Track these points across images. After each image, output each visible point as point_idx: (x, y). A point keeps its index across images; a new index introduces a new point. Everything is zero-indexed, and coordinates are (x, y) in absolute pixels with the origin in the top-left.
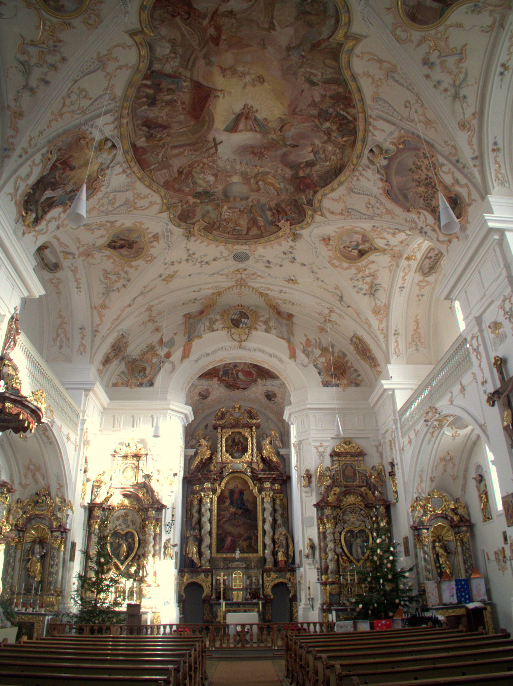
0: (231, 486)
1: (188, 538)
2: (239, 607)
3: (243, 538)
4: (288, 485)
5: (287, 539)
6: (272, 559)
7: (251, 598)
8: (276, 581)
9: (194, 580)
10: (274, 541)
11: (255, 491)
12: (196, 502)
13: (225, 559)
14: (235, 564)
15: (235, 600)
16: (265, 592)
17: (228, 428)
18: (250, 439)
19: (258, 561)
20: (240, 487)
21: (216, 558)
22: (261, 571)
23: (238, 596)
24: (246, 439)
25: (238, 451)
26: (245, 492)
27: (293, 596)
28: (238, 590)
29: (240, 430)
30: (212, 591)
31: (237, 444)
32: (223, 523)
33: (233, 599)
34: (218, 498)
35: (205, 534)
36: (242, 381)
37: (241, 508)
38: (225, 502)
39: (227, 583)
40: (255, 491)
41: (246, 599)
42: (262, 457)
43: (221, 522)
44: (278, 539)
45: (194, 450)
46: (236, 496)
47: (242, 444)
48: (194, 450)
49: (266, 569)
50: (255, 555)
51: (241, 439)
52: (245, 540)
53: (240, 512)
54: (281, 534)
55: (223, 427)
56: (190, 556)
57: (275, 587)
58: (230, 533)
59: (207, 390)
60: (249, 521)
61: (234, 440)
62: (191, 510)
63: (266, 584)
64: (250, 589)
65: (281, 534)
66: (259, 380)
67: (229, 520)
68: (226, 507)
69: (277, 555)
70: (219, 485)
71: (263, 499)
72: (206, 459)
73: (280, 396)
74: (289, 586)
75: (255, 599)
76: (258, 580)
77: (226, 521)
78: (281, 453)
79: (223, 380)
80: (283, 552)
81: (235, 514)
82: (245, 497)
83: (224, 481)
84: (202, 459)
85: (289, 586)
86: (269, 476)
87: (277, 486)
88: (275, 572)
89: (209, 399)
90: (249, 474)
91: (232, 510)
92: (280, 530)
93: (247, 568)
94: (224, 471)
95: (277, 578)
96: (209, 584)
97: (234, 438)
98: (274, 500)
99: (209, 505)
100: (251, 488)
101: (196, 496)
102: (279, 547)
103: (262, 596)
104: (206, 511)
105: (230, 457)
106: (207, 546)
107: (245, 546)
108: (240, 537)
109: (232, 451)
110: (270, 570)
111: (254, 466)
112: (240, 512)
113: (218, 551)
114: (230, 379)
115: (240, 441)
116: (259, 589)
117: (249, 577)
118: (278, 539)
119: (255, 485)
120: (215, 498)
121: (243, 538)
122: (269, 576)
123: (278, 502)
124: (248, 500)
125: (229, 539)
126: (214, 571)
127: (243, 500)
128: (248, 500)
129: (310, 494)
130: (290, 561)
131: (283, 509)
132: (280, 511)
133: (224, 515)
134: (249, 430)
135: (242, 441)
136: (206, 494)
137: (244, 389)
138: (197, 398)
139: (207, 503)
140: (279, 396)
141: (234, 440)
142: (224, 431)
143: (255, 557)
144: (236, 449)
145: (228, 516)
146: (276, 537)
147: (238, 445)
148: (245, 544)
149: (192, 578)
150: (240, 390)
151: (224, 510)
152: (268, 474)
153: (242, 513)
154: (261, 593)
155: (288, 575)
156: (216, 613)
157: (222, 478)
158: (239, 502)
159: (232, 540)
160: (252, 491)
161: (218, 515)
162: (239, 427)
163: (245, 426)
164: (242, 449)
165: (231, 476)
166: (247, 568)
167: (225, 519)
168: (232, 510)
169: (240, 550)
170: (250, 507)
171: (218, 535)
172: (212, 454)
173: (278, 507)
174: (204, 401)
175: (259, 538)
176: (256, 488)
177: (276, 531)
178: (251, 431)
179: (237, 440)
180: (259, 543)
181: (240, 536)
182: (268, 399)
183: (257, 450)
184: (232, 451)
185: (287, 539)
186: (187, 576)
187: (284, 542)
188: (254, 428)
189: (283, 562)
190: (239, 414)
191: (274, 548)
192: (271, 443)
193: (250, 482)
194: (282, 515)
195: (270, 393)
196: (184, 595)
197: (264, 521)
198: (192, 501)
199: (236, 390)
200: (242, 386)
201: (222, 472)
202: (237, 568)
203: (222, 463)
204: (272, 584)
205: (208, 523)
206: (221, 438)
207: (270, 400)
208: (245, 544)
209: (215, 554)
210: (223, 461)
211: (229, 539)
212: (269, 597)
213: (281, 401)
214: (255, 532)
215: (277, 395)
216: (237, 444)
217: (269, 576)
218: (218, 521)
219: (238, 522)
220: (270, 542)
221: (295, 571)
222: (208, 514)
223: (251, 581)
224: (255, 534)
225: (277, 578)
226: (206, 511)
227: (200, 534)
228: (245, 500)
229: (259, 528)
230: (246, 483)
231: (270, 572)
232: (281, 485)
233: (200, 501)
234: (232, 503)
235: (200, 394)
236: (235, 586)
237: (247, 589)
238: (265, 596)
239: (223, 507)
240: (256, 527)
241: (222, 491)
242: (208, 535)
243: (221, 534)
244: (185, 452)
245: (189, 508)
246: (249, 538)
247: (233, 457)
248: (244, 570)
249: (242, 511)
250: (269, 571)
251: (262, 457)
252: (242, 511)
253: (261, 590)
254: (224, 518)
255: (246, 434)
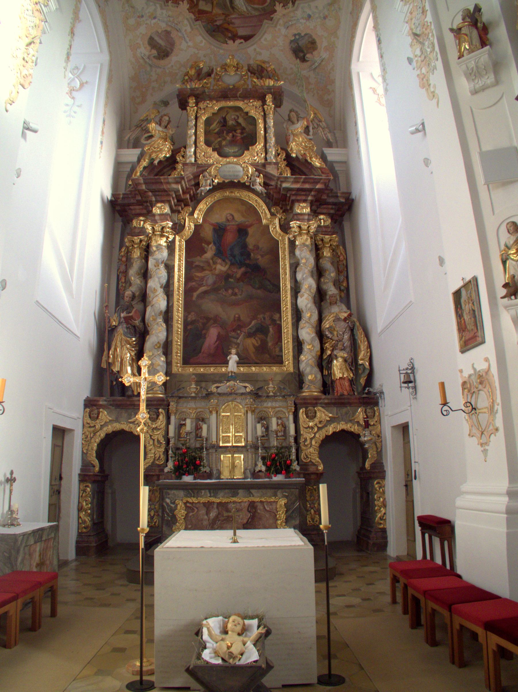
0: (219, 218)
1: (113, 330)
2: (235, 495)
3: (246, 330)
4: (346, 225)
5: (352, 330)
6: (319, 376)
7: (268, 469)
8: (331, 429)
9: (125, 427)
10: (321, 335)
11: (275, 229)
12: (137, 254)
13: (201, 379)
14: (224, 387)
15: (226, 476)
16: (302, 456)
17: (211, 99)
18: (260, 121)
19: (283, 382)
20: (239, 218)
21: (182, 375)
22: (290, 402)
23: (233, 466)
24: (253, 121)
25: (233, 142)
26: (250, 231)
27: (373, 466)
28: (236, 449)
29: (240, 104)
30: (166, 451)
31: (232, 130)
32: (199, 297)
33: (220, 473)
34: (189, 243)
35: (155, 320)
36: (242, 16)
37: (241, 264)
38: (203, 252)
39: (204, 433)
40: (275, 229)
41: (255, 474)
42: (288, 157)
43: (195, 294)
44: (331, 329)
45: (138, 151)
46: (230, 238)
47: (243, 129)
48: (138, 151)
49: (305, 398)
50: (275, 369)
51: (241, 120)
52: (250, 335)
53: (239, 272)
54: (337, 319)
55: (199, 97)
56: (116, 369)
57: (328, 440)
58: (216, 320)
59: (168, 33)
60: (260, 293)
61: (224, 123)
62: (125, 273)
63: (306, 435)
64: (264, 448)
65: (337, 319)
66: (278, 7)
67: (215, 290)
68: (208, 262)
69: (329, 367)
70: (192, 214)
71: (292, 244)
72: (160, 162)
73: (325, 44)
74: (362, 439)
75: (277, 472)
76: (285, 427)
77: (206, 292)
78: (330, 158)
79: (201, 12)
80: (345, 360)
81: (227, 277)
82: (251, 241)
83: (203, 206)
84: (152, 161)
85: (362, 439)
86: (307, 186)
87: (324, 220)
88: (326, 406)
89: (173, 59)
90: (259, 188)
91: (221, 267)
92: (335, 309)
93: (256, 395)
94: (202, 182)
95: (332, 420)
96: (159, 435)
97: (224, 119)
98: (317, 249)
99: (165, 253)
100: (264, 222)
101: (136, 239)
102: (334, 348)
103: (295, 466)
104: (157, 265)
105: (216, 155)
106: (156, 346)
107: (252, 350)
108: (240, 327)
109: (220, 143)
110: (314, 402)
111: (271, 170)
112: (239, 272)
113: (186, 361)
114: (217, 11)
115: (239, 124)
116: (289, 448)
117: (262, 419)
118: (331, 329)
119: (272, 214)
120: (180, 243)
121: (246, 330)
122: (311, 417)
123: (327, 253)
124: (257, 247)
125: (213, 333)
126: (173, 405)
127: (245, 246)
128: (257, 247)
129: (490, 79)
130: (362, 381)
131: (339, 272)
132: (331, 274)
133: (202, 279)
134: (258, 103)
135: (243, 124)
136: (157, 228)
137: (247, 38)
138: (144, 50)
139: (159, 246)
140: (322, 44)
141: (224, 123)
142: (201, 105)
143: (276, 374)
144: (228, 138)
145: (211, 280)
146: (326, 325)
147: (235, 131)
148: (251, 343)
149: (117, 420)
150: (238, 41)
151: (202, 269)
152: (304, 182)
153: (245, 274)
154: (294, 457)
155: (360, 414)
156: (173, 510)
157: (196, 200)
158: (237, 251)
159: (219, 337)
160: (267, 227)
161: (188, 278)
162: (235, 97)
163: (247, 95)
164: (242, 138)
165: (218, 195)
166: (256, 395)
167: (203, 289)
168: (221, 267)
169: (237, 354)
170: (263, 261)
171: (186, 324)
172: (175, 152)
173: (326, 264)
174: (162, 62)
175: (284, 330)
176: (277, 221)
177: (325, 313)
178: (264, 102)
179: (231, 123)
180: (284, 341)
181: (238, 325)
182: (297, 57)
183: (277, 142)
184: (220, 143)
185: (352, 330)
186: (104, 415)
187: (346, 337)
188: (269, 98)
189: (347, 384)
190: (237, 78)
191: (322, 350)
192: (307, 130)
193: (262, 208)
194: (337, 283)
195: (302, 43)
196: (96, 462)
197: (296, 290)
198: (128, 252)
199: (230, 42)
200: (241, 32)
201: (197, 185)
202: (232, 394)
203: (199, 166)
204: (321, 435)
205: (160, 292)
206: (196, 118)
207: (303, 60)
208: (251, 343)
209: (177, 368)
210: (199, 162)
211: (213, 333)
212: (312, 469)
213: (325, 55)
214: (276, 316)
215: (318, 41)
216: (232, 130)
217: (311, 417)
218: (188, 292)
219: (235, 294)
220: (314, 335)
221: (376, 404)
222: (163, 273)
223: (267, 428)
224: (273, 321)
225: (332, 420)
226: (157, 265)
227: (143, 320)
228: (251, 247)
229: (283, 308)
230: (252, 211)
231: (315, 405)
232: (332, 217)
233: (147, 251)
234: (220, 253)
235: (152, 43)
236: (226, 439)
237: (256, 448)
238: (304, 466)
239: (198, 261)
240: (277, 307)
241: (197, 227)
242: (160, 320)
243: (193, 322)
244: (117, 156)
245: (123, 268)
246: (262, 330)
247: (220, 155)
248: (249, 400)
249: (243, 269)
250: (314, 402)
251: (288, 157)
252: (243, 269)
253: (294, 450)
254: (201, 285)
255: (252, 113)
